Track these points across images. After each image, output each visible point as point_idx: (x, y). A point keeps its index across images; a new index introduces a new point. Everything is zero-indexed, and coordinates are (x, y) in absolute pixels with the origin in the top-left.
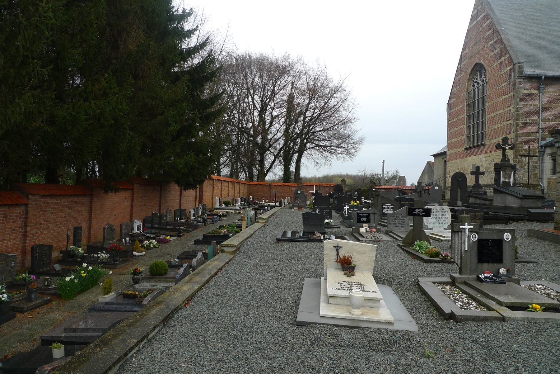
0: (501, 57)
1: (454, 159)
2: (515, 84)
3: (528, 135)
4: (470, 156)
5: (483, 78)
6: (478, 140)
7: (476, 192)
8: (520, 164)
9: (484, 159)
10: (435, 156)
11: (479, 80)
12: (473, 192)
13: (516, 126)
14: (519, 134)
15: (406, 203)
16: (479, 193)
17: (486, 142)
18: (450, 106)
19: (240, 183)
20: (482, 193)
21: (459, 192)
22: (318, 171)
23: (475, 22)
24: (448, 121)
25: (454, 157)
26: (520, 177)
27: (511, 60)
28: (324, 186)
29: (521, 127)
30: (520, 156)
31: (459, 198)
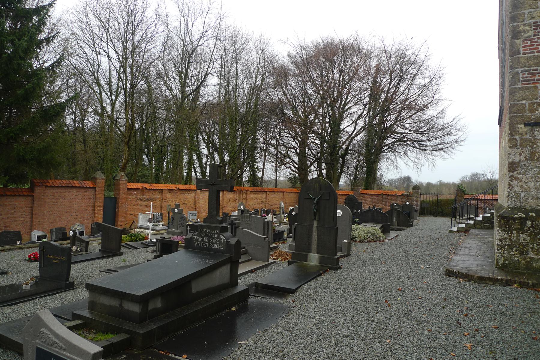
7: (203, 245)
8: (527, 150)
12: (196, 244)
13: (512, 38)
14: (523, 60)
15: (54, 259)
16: (211, 246)
19: (266, 192)
20: (220, 247)
21: (315, 229)
22: (419, 173)
26: (528, 190)
28: (388, 195)
29: (527, 39)
30: (526, 125)
31: (314, 246)
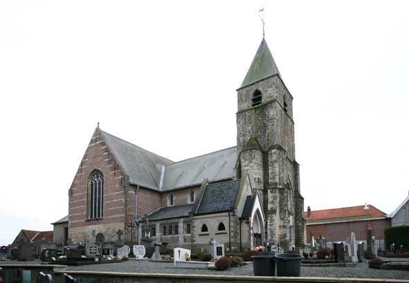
0: (115, 170)
1: (76, 227)
2: (125, 187)
3: (131, 216)
4: (90, 225)
5: (99, 179)
6: (95, 215)
9: (102, 227)
10: (55, 224)
11: (96, 180)
17: (105, 217)
18: (71, 192)
23: (94, 144)
24: (70, 201)
25: (74, 225)
27: (122, 174)
